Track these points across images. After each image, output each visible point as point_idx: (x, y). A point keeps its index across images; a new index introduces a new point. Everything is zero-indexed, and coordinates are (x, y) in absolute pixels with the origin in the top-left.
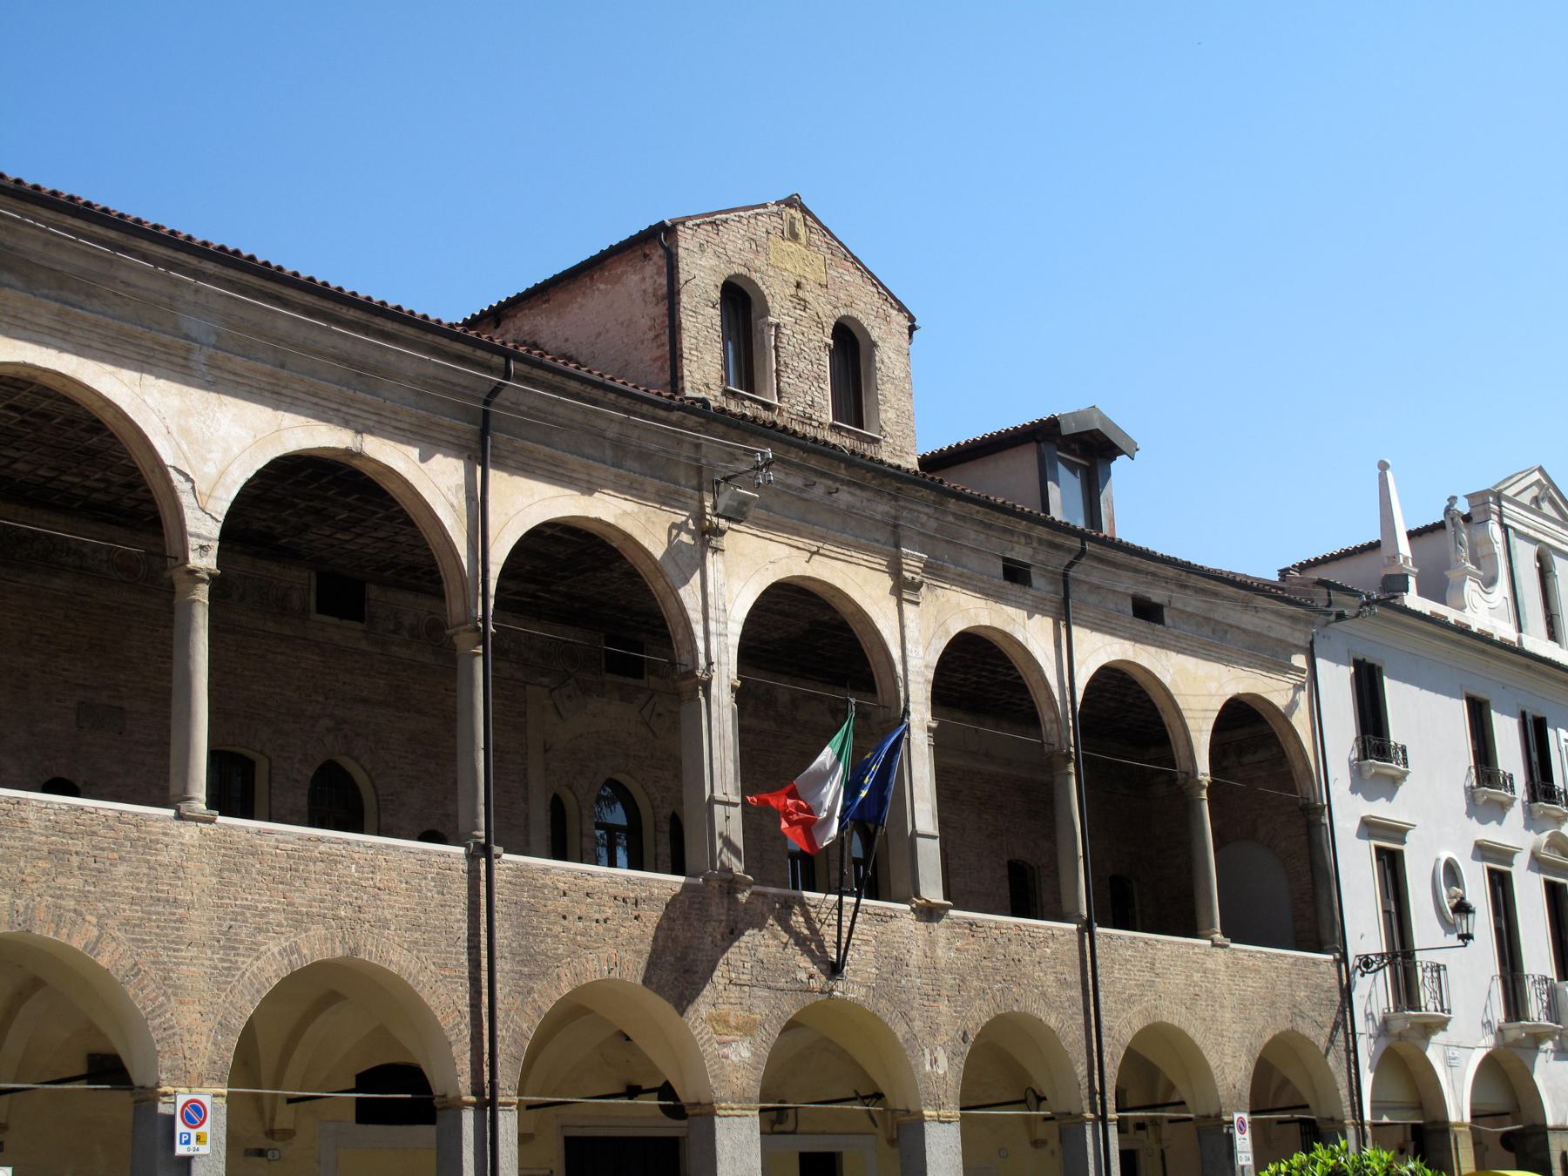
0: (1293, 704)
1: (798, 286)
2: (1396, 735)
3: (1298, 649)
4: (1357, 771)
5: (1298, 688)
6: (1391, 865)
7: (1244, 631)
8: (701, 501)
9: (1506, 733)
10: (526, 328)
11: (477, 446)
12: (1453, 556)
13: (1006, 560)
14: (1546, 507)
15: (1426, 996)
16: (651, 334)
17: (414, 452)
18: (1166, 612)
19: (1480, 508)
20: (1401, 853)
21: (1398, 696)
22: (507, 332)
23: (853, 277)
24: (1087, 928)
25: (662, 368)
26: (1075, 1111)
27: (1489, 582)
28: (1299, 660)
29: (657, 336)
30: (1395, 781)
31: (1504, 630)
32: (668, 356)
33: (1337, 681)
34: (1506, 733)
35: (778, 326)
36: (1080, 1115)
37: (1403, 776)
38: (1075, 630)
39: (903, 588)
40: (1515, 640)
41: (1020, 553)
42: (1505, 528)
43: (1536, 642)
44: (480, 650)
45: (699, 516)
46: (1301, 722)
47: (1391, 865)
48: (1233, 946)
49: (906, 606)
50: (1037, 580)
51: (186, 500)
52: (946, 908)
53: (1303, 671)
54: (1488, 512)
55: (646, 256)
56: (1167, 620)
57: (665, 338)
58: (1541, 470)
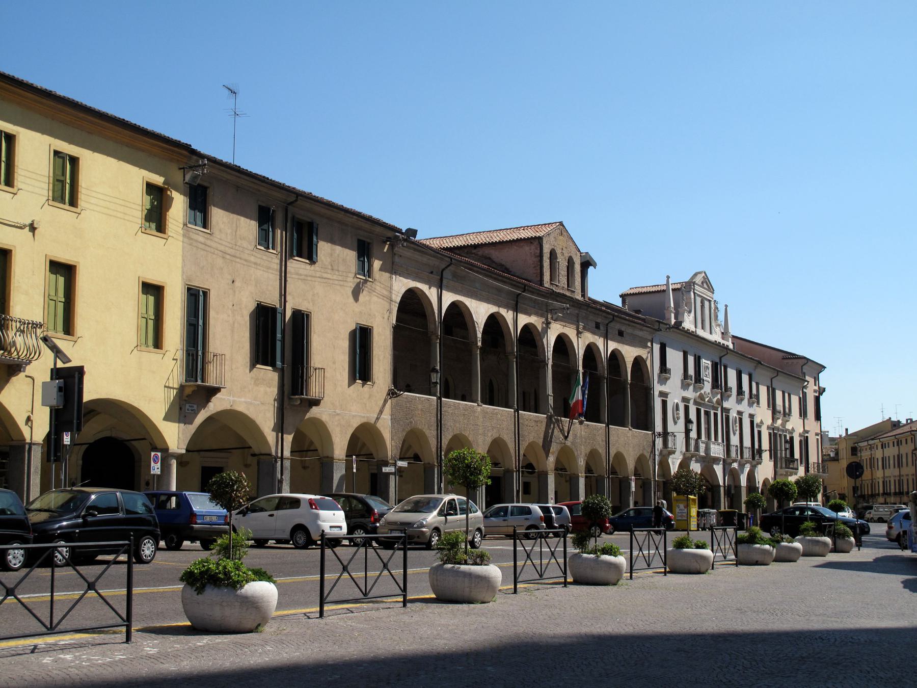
0: (647, 357)
1: (562, 249)
2: (668, 366)
3: (649, 341)
4: (659, 377)
5: (648, 352)
6: (664, 403)
7: (639, 337)
8: (548, 315)
9: (691, 359)
10: (486, 252)
11: (515, 307)
12: (681, 304)
13: (596, 322)
14: (705, 285)
15: (670, 445)
16: (533, 266)
17: (506, 310)
18: (625, 333)
19: (688, 287)
20: (667, 401)
21: (669, 351)
22: (479, 251)
23: (571, 244)
24: (608, 425)
25: (537, 276)
26: (602, 475)
27: (690, 312)
28: (649, 344)
29: (535, 267)
30: (667, 379)
31: (692, 328)
32: (539, 273)
33: (657, 348)
34: (691, 359)
35: (559, 262)
36: (604, 476)
37: (669, 378)
38: (609, 341)
39: (579, 333)
40: (694, 331)
41: (599, 320)
42: (694, 293)
43: (700, 332)
44: (515, 360)
45: (547, 319)
46: (648, 363)
47: (664, 403)
48: (633, 430)
49: (579, 339)
50: (601, 327)
51: (477, 329)
52: (584, 421)
53: (650, 347)
54: (691, 288)
55: (531, 243)
56: (624, 336)
57: (538, 268)
58: (705, 273)
